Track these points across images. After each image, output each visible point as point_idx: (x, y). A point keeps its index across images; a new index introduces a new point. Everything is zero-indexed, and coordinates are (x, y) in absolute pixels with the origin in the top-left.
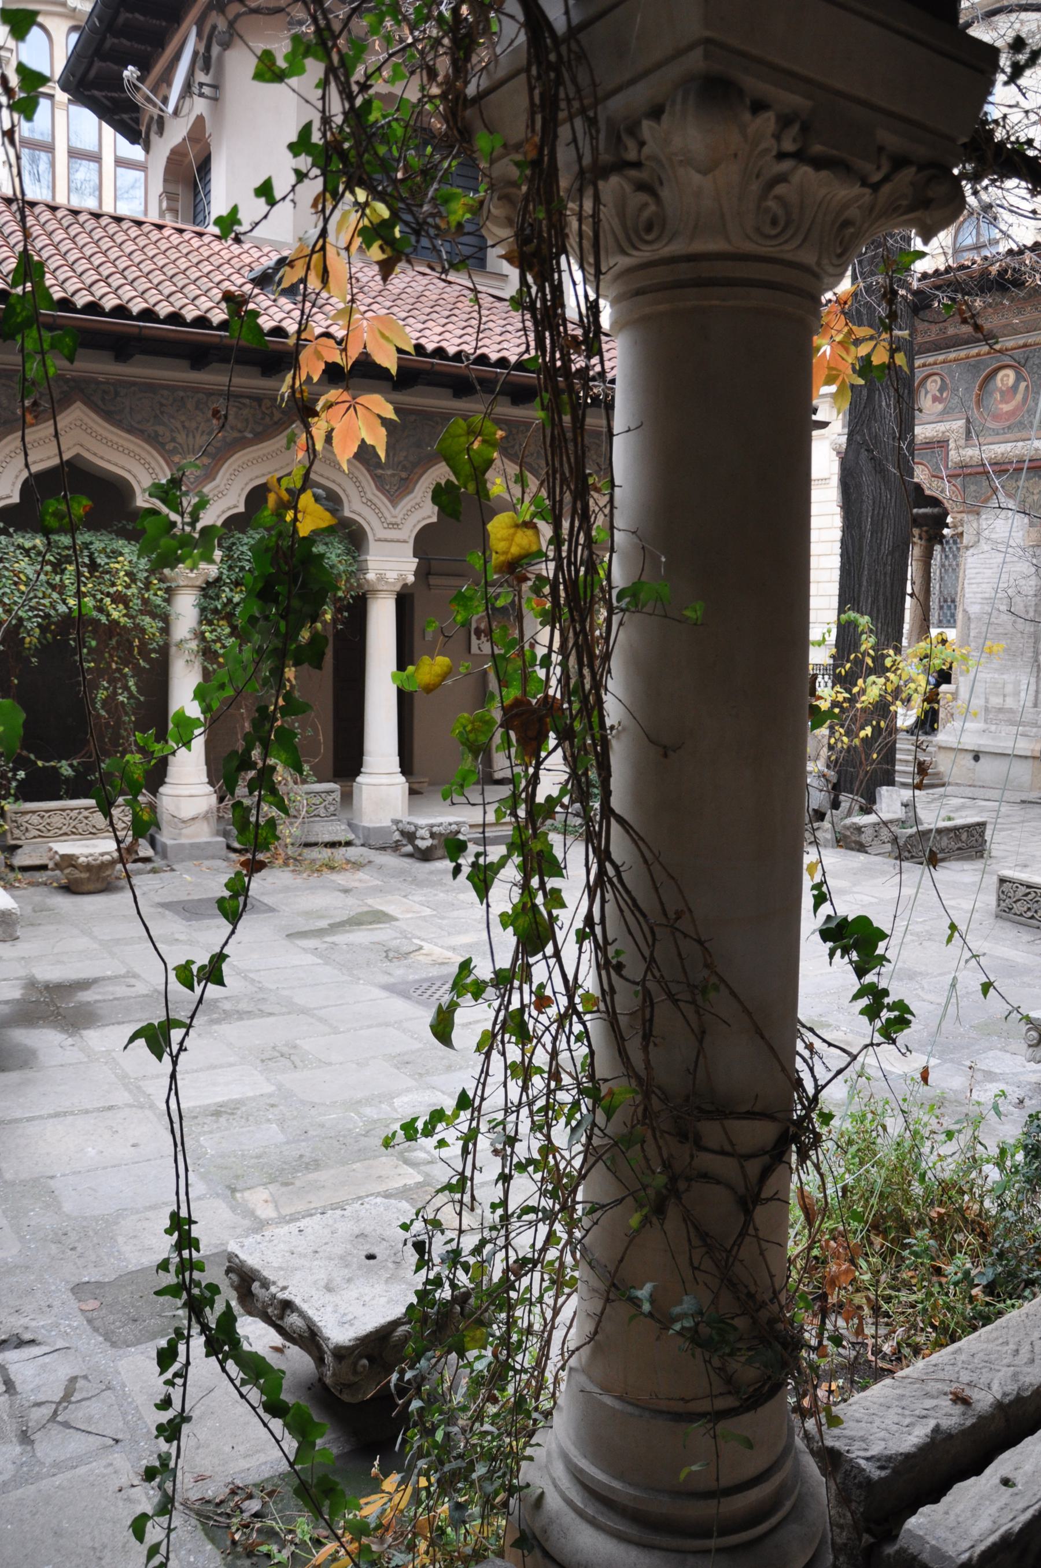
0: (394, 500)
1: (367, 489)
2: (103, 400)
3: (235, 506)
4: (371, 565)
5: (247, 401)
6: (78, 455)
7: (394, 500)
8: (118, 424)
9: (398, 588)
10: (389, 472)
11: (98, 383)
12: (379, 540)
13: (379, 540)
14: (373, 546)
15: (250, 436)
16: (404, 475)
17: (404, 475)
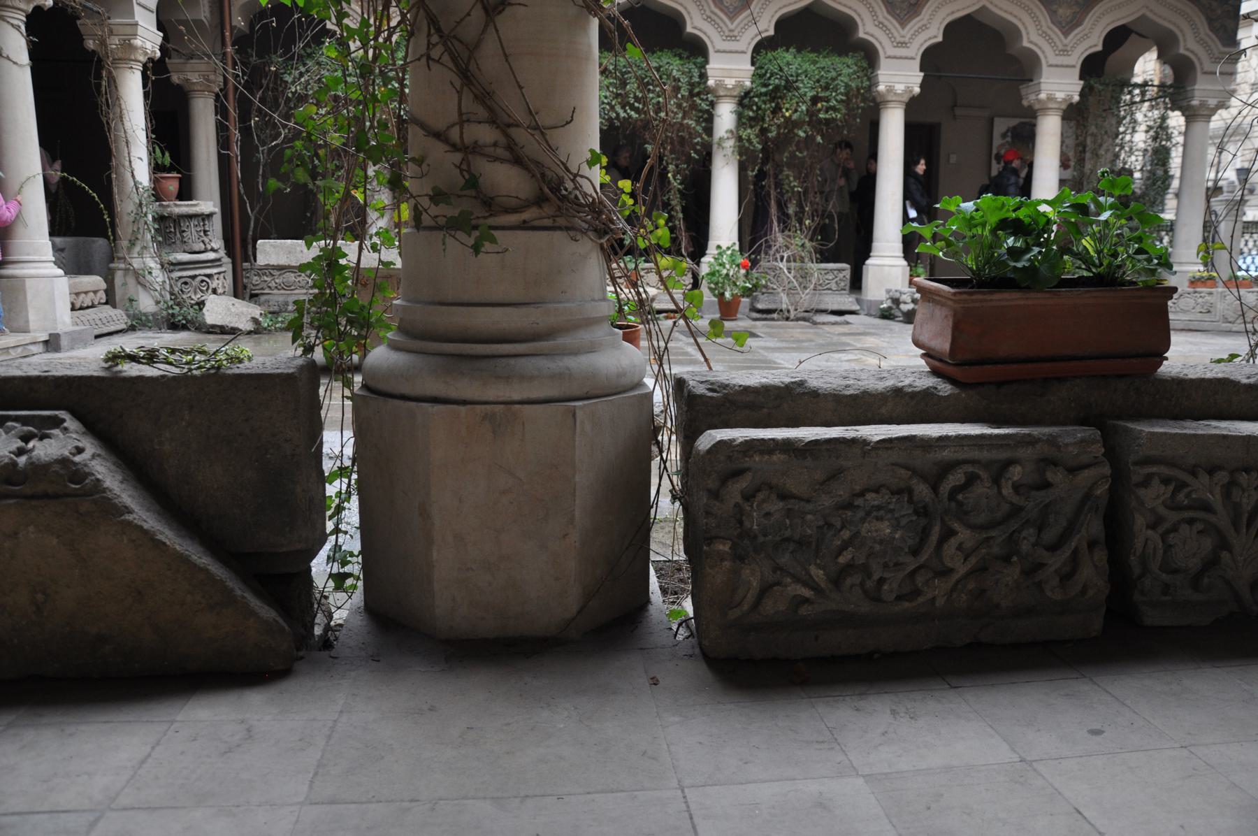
0: (903, 24)
1: (879, 14)
4: (881, 78)
7: (903, 24)
9: (906, 99)
12: (889, 57)
13: (889, 57)
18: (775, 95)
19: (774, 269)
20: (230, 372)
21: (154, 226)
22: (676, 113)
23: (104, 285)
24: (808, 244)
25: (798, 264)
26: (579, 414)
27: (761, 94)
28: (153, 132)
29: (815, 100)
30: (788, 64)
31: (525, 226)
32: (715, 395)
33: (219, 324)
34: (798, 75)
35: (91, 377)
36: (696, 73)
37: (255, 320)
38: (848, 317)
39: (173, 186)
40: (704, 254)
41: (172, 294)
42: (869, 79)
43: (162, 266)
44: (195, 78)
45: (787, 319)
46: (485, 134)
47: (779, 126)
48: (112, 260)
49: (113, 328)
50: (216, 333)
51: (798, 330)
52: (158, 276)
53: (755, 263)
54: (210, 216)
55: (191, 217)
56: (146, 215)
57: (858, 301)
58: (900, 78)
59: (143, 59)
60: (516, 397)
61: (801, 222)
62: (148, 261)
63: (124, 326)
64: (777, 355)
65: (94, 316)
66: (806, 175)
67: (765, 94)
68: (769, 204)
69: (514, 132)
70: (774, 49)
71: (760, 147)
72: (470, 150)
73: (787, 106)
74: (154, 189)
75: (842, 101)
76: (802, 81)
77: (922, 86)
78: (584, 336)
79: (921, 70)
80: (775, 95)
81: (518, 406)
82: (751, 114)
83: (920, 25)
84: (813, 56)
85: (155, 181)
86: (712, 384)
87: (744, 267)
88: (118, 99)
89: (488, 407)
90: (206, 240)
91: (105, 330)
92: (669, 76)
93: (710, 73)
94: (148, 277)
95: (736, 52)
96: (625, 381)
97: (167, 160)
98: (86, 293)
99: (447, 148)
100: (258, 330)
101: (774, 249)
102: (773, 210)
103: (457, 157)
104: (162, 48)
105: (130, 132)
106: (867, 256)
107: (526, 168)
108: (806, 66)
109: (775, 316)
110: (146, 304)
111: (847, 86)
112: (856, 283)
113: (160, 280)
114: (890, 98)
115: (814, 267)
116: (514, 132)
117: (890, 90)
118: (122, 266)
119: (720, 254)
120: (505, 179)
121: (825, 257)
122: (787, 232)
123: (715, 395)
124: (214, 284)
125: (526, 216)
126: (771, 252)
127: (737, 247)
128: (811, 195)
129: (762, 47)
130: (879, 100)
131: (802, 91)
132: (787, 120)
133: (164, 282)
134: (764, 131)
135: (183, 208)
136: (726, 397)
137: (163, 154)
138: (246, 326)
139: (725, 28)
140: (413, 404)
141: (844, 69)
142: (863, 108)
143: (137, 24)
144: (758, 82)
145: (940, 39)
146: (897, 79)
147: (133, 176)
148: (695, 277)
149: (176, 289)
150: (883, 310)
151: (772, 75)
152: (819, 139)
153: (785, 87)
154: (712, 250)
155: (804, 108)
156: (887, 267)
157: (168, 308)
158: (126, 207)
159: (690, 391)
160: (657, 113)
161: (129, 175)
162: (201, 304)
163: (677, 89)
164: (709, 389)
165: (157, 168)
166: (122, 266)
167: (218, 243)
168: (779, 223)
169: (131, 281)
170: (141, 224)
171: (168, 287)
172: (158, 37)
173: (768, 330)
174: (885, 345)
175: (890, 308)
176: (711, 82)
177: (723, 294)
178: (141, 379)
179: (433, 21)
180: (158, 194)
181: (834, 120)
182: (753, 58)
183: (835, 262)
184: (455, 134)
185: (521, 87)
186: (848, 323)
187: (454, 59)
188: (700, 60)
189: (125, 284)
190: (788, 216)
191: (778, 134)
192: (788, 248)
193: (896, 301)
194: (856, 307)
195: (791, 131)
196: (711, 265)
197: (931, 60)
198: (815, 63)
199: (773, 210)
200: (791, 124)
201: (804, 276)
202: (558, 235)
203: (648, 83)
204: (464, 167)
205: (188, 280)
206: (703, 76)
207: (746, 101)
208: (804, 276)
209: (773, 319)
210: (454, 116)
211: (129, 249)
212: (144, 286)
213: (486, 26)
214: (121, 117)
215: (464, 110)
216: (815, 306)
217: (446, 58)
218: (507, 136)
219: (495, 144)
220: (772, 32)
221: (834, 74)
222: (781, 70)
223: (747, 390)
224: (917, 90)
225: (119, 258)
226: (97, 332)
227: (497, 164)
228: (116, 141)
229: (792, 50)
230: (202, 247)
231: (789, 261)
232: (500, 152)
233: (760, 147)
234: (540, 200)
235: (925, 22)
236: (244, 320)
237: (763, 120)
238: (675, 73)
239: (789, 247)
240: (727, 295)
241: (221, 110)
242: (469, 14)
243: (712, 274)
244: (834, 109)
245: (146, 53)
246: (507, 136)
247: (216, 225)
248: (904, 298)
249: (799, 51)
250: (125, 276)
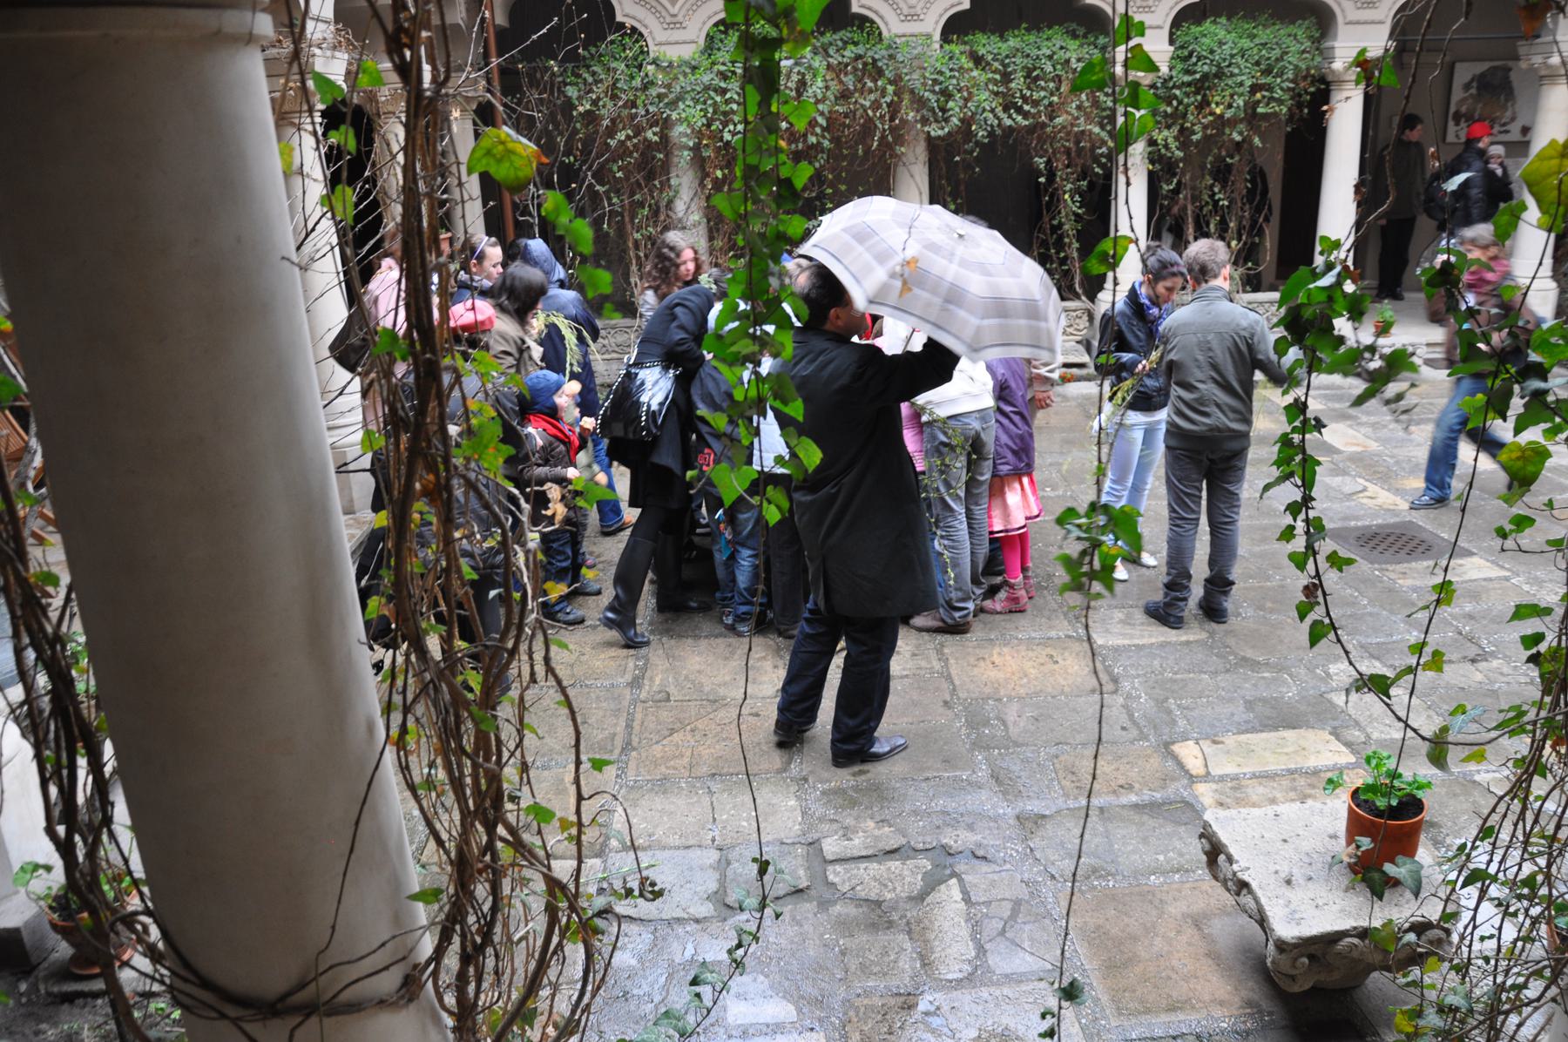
18: (1202, 86)
67: (1189, 84)
73: (1217, 98)
80: (1202, 86)
142: (1312, 94)
144: (1180, 66)
151: (1199, 59)
182: (1171, 34)
203: (1037, 78)
229: (1223, 20)
237: (1184, 116)
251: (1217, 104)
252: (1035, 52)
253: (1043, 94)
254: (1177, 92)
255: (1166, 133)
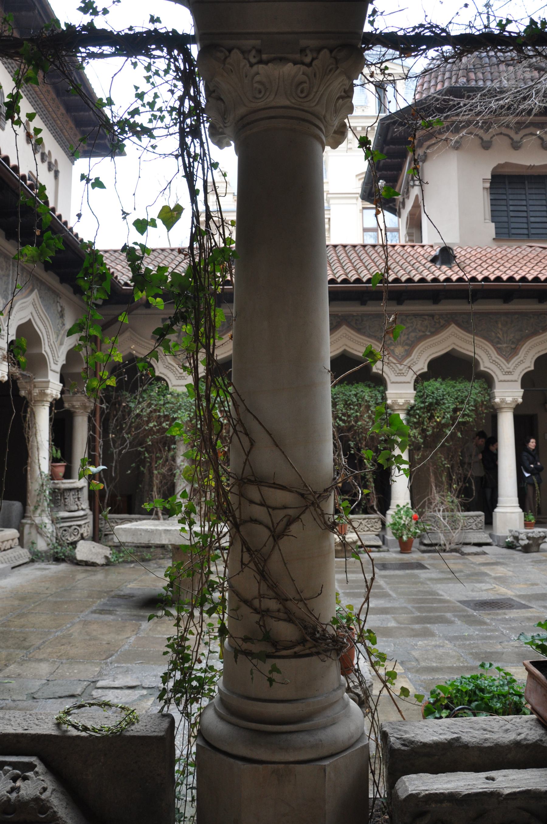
0: (508, 361)
1: (492, 355)
2: (356, 323)
3: (423, 369)
5: (426, 317)
6: (345, 350)
7: (508, 361)
8: (364, 334)
9: (513, 406)
10: (505, 345)
11: (353, 316)
12: (501, 381)
13: (501, 381)
14: (497, 384)
15: (428, 333)
16: (513, 346)
17: (513, 346)
18: (430, 408)
19: (434, 517)
20: (128, 734)
21: (49, 498)
22: (368, 422)
23: (18, 535)
24: (456, 501)
25: (450, 514)
26: (328, 770)
27: (421, 408)
28: (53, 441)
29: (455, 410)
30: (437, 389)
31: (296, 656)
32: (406, 748)
33: (85, 559)
34: (444, 395)
35: (51, 735)
36: (379, 396)
37: (106, 558)
38: (485, 549)
39: (61, 471)
40: (388, 508)
41: (57, 539)
42: (489, 395)
43: (53, 522)
44: (77, 404)
45: (444, 551)
46: (273, 605)
47: (433, 428)
48: (24, 516)
49: (21, 562)
50: (82, 565)
51: (453, 561)
52: (50, 528)
53: (421, 514)
54: (81, 489)
55: (70, 490)
56: (45, 491)
57: (491, 536)
58: (509, 393)
59: (50, 400)
60: (291, 759)
61: (450, 486)
62: (44, 519)
63: (27, 560)
64: (439, 586)
65: (12, 555)
66: (453, 457)
67: (424, 408)
68: (429, 475)
69: (289, 604)
70: (428, 380)
71: (422, 441)
72: (264, 613)
73: (438, 414)
74: (51, 475)
75: (473, 410)
76: (447, 399)
77: (523, 397)
78: (329, 713)
79: (522, 388)
80: (430, 408)
81: (291, 766)
82: (415, 420)
83: (519, 360)
84: (452, 382)
85: (52, 469)
86: (404, 740)
87: (415, 519)
88: (35, 424)
89: (275, 766)
90: (79, 503)
91: (17, 563)
92: (363, 398)
93: (388, 396)
94: (44, 529)
95: (404, 383)
96: (353, 740)
97: (59, 455)
98: (8, 541)
99: (252, 611)
100: (108, 563)
101: (434, 504)
102: (432, 479)
103: (257, 617)
104: (62, 392)
105: (40, 443)
106: (495, 507)
107: (296, 625)
108: (449, 389)
109: (437, 548)
110: (42, 545)
111: (475, 400)
112: (489, 522)
113: (50, 530)
114: (503, 406)
115: (461, 515)
116: (289, 604)
117: (503, 401)
118: (29, 522)
119: (399, 511)
120: (285, 631)
121: (467, 508)
122: (441, 493)
123: (406, 748)
124: (82, 531)
125: (296, 649)
126: (432, 507)
127: (410, 506)
128: (456, 469)
129: (421, 379)
130: (496, 407)
131: (447, 405)
132: (439, 423)
133: (53, 531)
134: (424, 431)
135: (66, 484)
136: (413, 750)
137: (57, 451)
138: (101, 561)
139: (396, 369)
140: (232, 760)
141: (472, 390)
142: (486, 413)
143: (49, 382)
144: (419, 400)
145: (532, 368)
146: (507, 394)
147: (40, 468)
148: (383, 524)
149: (59, 534)
150: (509, 542)
151: (427, 396)
152: (459, 434)
153: (436, 404)
154: (393, 506)
155: (449, 416)
156: (509, 511)
157: (55, 548)
158: (34, 486)
159: (391, 747)
160: (356, 422)
161: (37, 468)
162: (74, 544)
163: (368, 407)
164: (402, 744)
165: (54, 460)
166: (29, 522)
167: (85, 505)
168: (436, 486)
169: (34, 531)
170: (42, 497)
171: (55, 534)
172: (60, 386)
173: (432, 562)
174: (510, 574)
175: (512, 542)
176: (389, 402)
177: (401, 537)
178: (78, 737)
179: (244, 543)
180: (53, 476)
181: (468, 422)
182: (415, 386)
183: (474, 511)
184: (256, 603)
185: (293, 580)
186: (485, 553)
187: (256, 565)
188: (382, 388)
189: (30, 533)
190: (442, 482)
191: (433, 432)
192: (442, 503)
193: (517, 538)
194: (489, 541)
195: (441, 430)
196: (393, 516)
197: (527, 381)
198: (454, 387)
199: (432, 479)
200: (441, 427)
201: (454, 522)
202: (315, 658)
203: (350, 404)
204: (261, 623)
205: (67, 528)
206: (384, 398)
207: (412, 412)
208: (454, 522)
209: (435, 551)
210: (256, 593)
211: (34, 512)
212: (41, 534)
213: (274, 547)
214: (36, 434)
215: (261, 592)
216: (462, 541)
217: (252, 565)
218: (285, 608)
219: (279, 611)
220: (426, 370)
221: (466, 393)
222: (433, 393)
223: (425, 745)
224: (520, 400)
225: (27, 517)
226: (13, 565)
227: (280, 622)
228: (32, 448)
229: (439, 380)
230: (76, 508)
231: (444, 511)
232: (282, 615)
233: (422, 441)
234: (303, 642)
235: (522, 358)
236: (100, 557)
237: (423, 423)
238: (367, 398)
239: (443, 505)
240: (405, 538)
241: (92, 428)
242: (265, 545)
243: (394, 524)
244: (468, 415)
245: (52, 397)
246: (285, 608)
247: (85, 492)
248: (521, 536)
249: (443, 379)
250: (30, 527)
251: (438, 417)
252: (348, 393)
253: (352, 411)
254: (418, 411)
255: (414, 431)
